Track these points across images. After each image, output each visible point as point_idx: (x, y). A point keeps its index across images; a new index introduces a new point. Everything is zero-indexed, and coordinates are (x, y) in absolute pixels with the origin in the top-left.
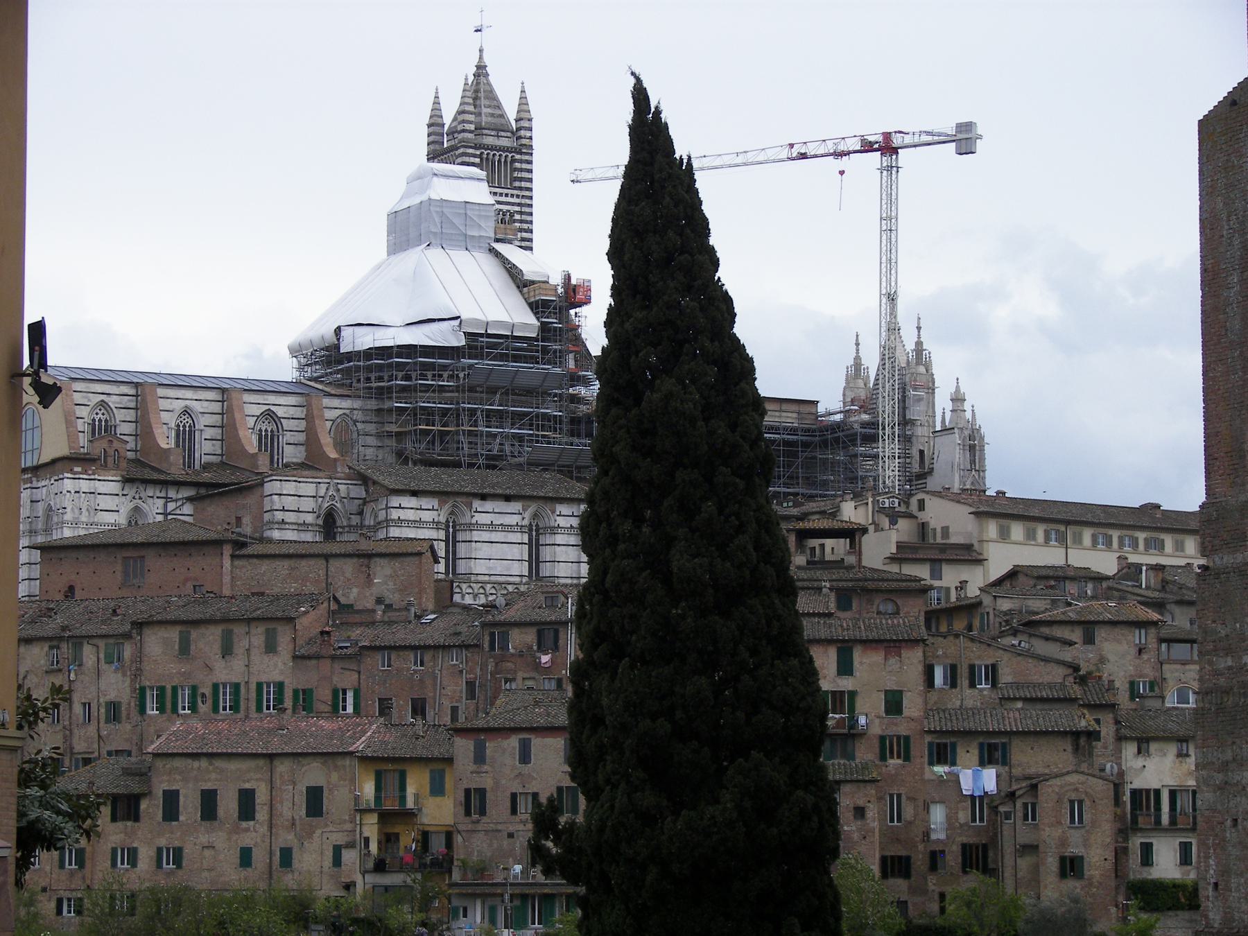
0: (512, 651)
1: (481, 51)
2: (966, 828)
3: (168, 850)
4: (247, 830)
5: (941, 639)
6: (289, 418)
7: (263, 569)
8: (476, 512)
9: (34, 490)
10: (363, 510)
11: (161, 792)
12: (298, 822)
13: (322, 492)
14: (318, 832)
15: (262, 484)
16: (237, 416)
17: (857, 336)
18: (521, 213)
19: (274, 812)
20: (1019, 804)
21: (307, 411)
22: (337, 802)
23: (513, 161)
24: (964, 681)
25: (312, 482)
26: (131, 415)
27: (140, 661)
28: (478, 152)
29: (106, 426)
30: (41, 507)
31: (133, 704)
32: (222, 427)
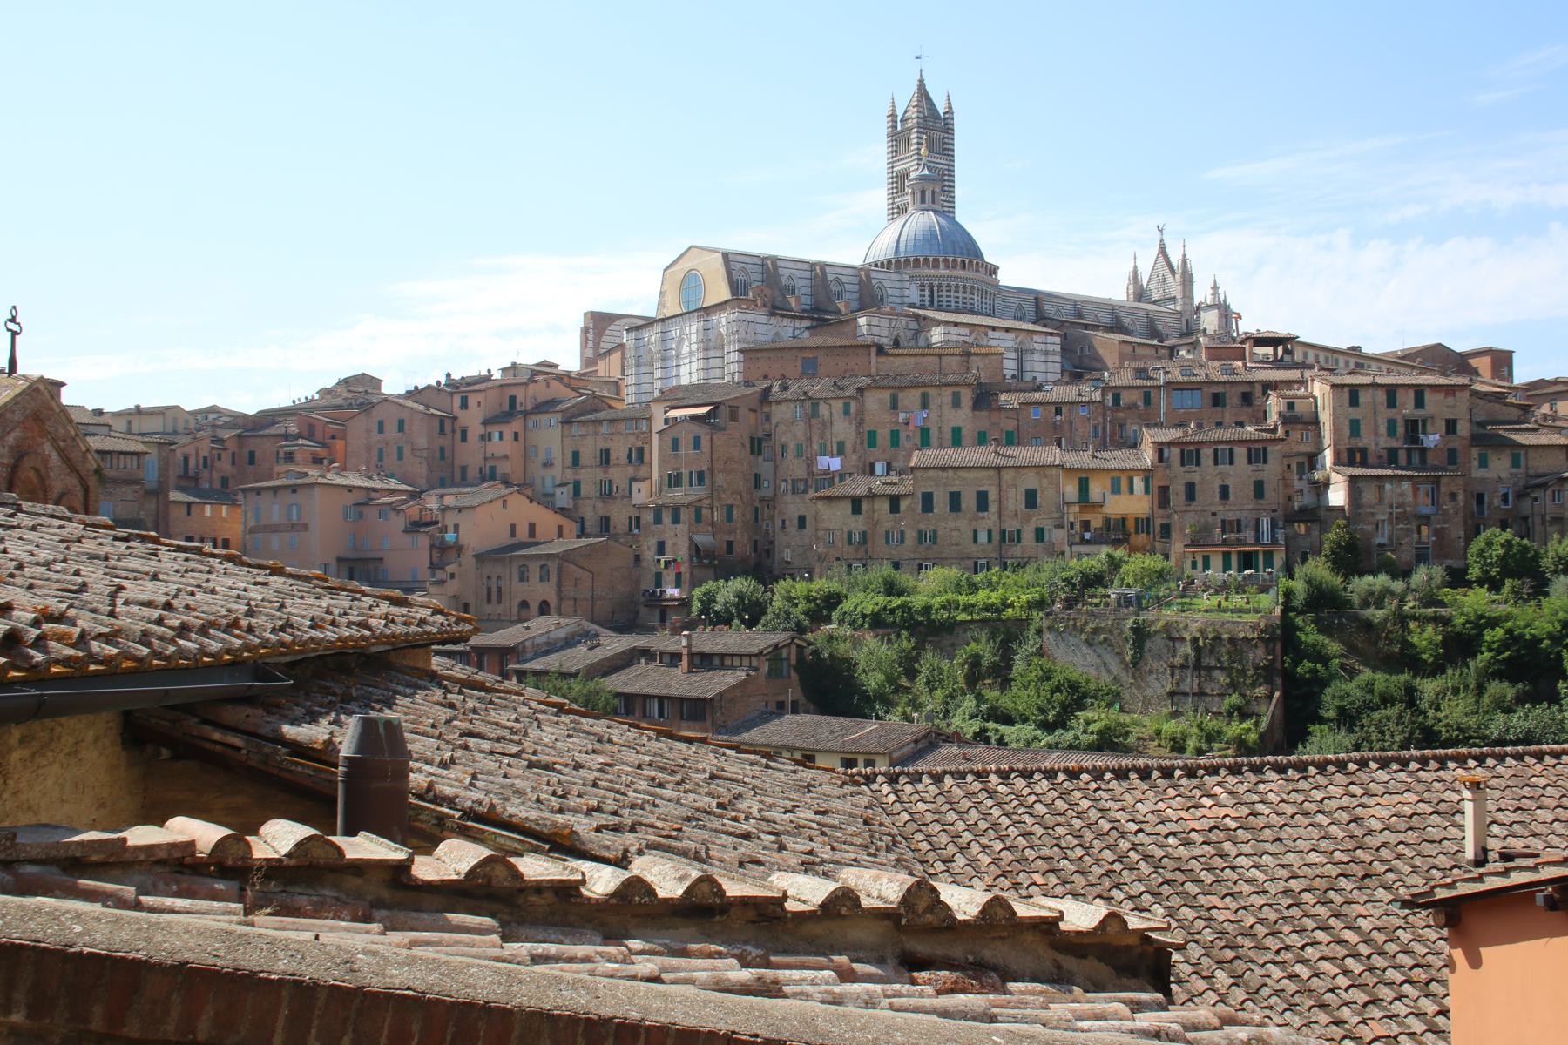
26: (759, 277)
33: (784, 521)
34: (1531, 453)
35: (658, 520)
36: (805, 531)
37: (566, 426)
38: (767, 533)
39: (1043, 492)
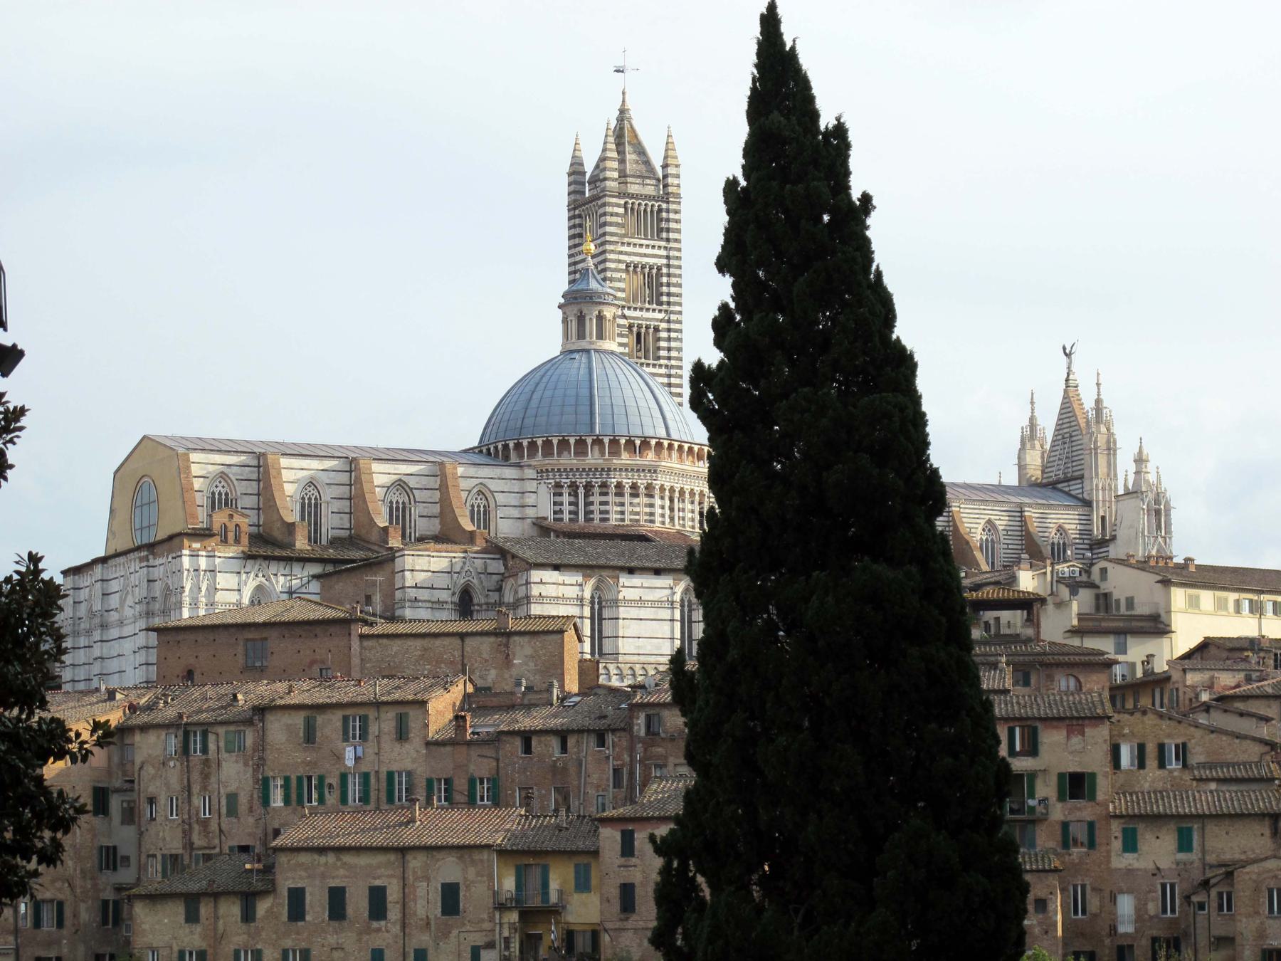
1: (624, 93)
2: (1156, 920)
3: (294, 952)
4: (379, 930)
5: (1127, 716)
6: (421, 489)
7: (395, 649)
8: (623, 586)
9: (151, 569)
10: (501, 587)
11: (286, 888)
12: (433, 923)
14: (455, 932)
15: (393, 559)
16: (366, 487)
17: (1032, 394)
18: (668, 266)
19: (407, 911)
20: (1213, 893)
21: (441, 481)
22: (475, 898)
23: (660, 210)
24: (1151, 762)
25: (446, 557)
26: (253, 487)
27: (263, 750)
28: (622, 202)
29: (226, 500)
30: (158, 588)
31: (255, 796)
32: (350, 499)
34: (1211, 828)
39: (468, 887)
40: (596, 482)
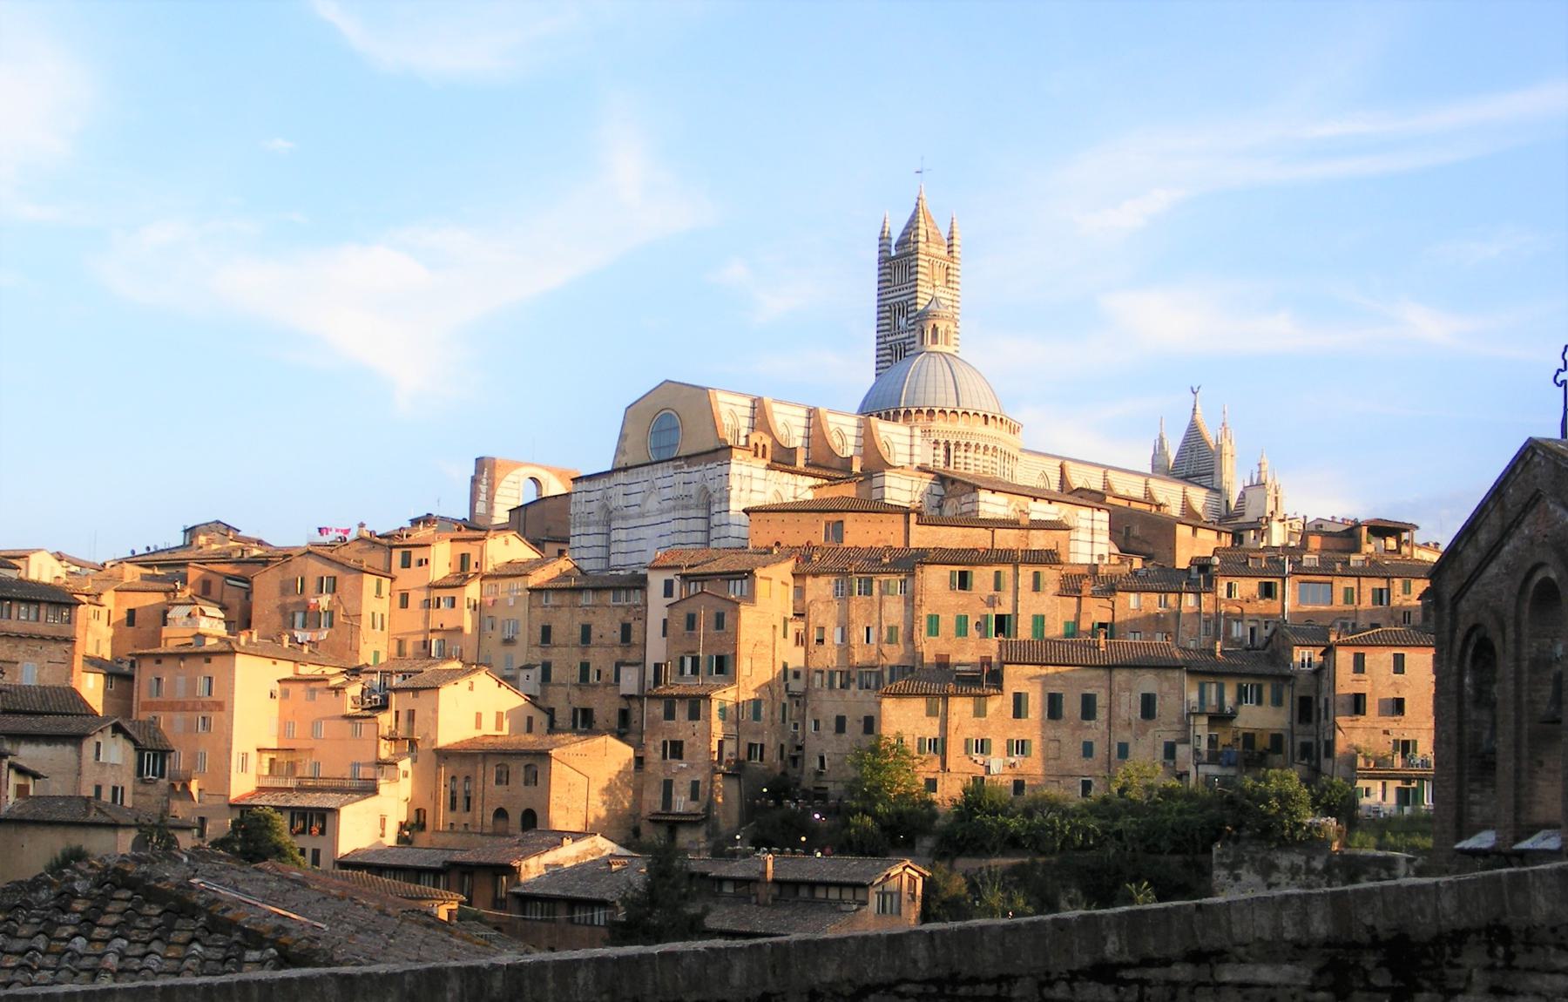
0: (1238, 597)
4: (1089, 727)
12: (1133, 723)
13: (915, 489)
14: (1151, 731)
18: (953, 307)
22: (1167, 707)
23: (947, 268)
28: (927, 258)
33: (817, 722)
35: (670, 715)
36: (844, 735)
37: (534, 594)
38: (795, 736)
40: (963, 442)
